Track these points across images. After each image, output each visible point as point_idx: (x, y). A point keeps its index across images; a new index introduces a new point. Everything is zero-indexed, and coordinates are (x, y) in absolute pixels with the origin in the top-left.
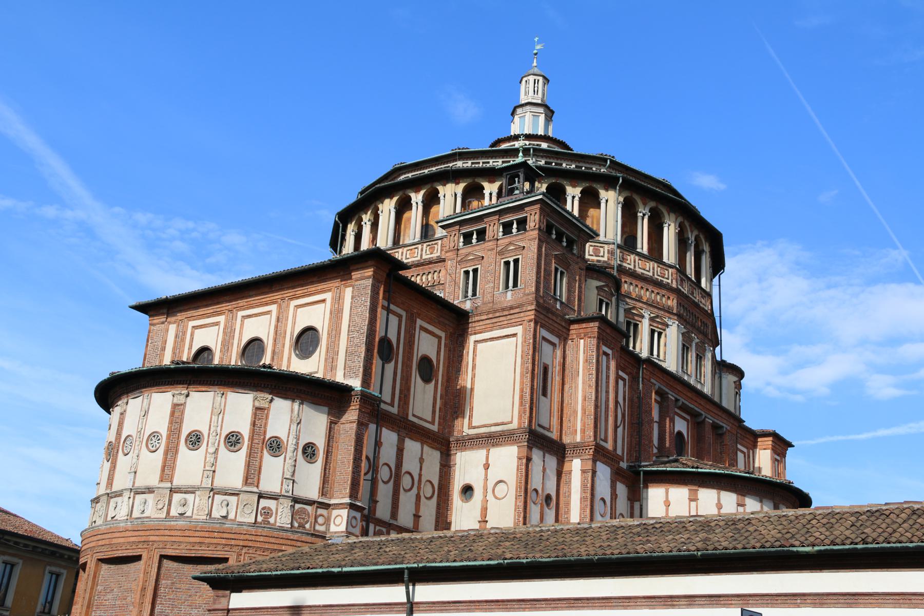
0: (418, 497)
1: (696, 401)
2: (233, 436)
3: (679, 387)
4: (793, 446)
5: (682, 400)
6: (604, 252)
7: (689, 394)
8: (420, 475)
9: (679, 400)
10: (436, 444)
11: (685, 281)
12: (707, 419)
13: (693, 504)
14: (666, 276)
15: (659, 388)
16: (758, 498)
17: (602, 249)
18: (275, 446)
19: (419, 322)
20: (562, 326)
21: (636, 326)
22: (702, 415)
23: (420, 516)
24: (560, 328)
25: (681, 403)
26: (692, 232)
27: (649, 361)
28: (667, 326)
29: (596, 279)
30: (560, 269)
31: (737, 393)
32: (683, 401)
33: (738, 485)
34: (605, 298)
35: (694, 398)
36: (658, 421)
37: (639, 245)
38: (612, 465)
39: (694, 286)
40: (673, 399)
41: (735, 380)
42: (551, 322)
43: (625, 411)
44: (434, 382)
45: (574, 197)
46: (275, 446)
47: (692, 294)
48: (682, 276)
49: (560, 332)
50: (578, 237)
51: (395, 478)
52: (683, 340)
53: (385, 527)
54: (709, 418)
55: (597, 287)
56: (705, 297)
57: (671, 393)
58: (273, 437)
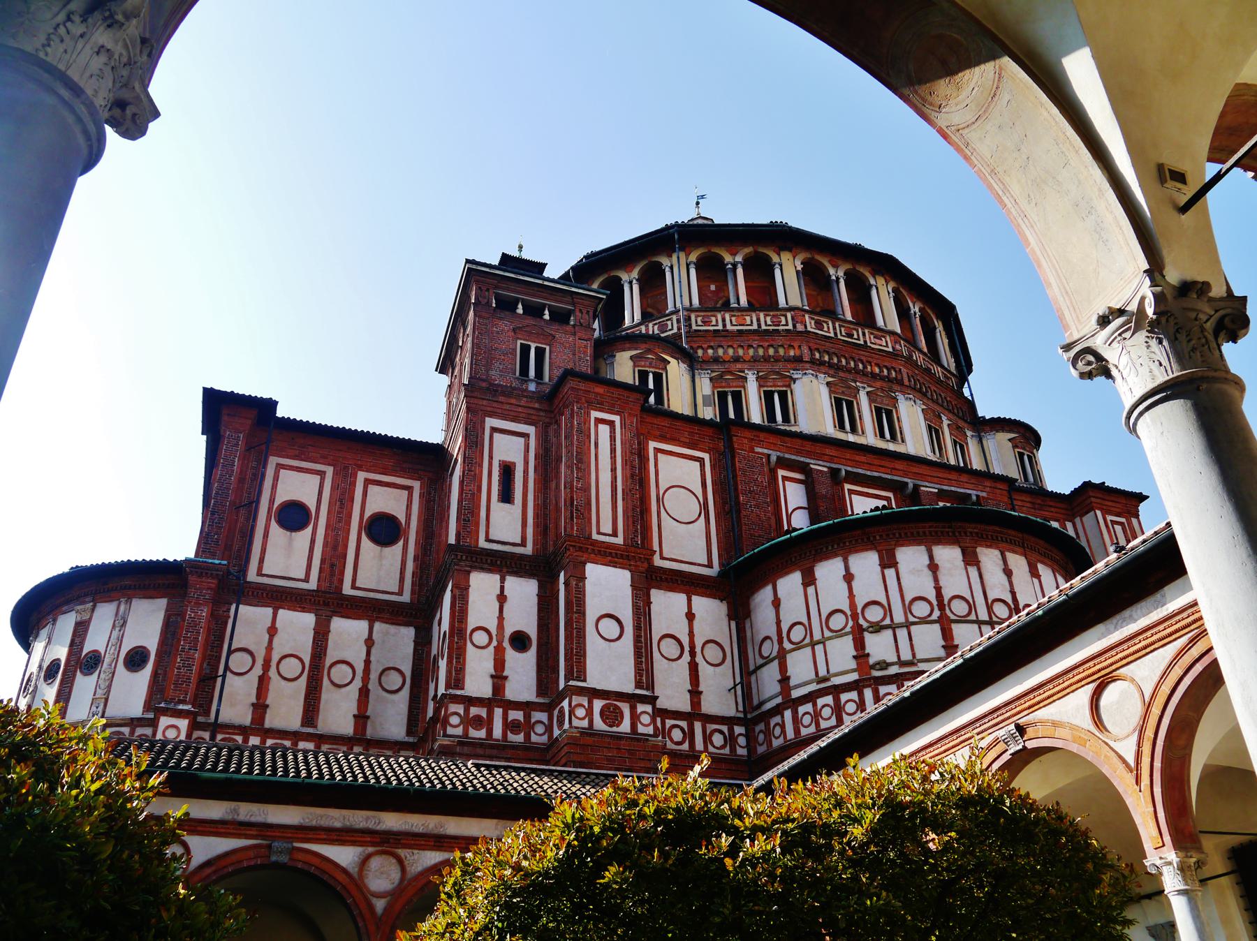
0: (364, 693)
1: (883, 467)
2: (54, 665)
4: (1147, 497)
5: (844, 469)
6: (672, 324)
7: (863, 459)
8: (367, 662)
10: (401, 618)
11: (826, 322)
12: (922, 488)
13: (811, 590)
14: (784, 322)
15: (778, 458)
16: (923, 548)
17: (669, 323)
18: (92, 663)
19: (361, 476)
20: (534, 408)
21: (737, 397)
22: (907, 483)
23: (368, 717)
24: (532, 412)
25: (843, 473)
26: (836, 267)
27: (768, 431)
28: (795, 380)
29: (629, 349)
30: (533, 346)
31: (1021, 455)
32: (849, 469)
33: (875, 537)
34: (649, 367)
35: (876, 462)
36: (806, 506)
37: (732, 300)
38: (630, 565)
39: (852, 326)
40: (825, 469)
41: (1010, 437)
42: (508, 407)
43: (705, 498)
44: (401, 543)
45: (631, 283)
46: (92, 663)
47: (851, 336)
48: (816, 318)
49: (534, 417)
50: (573, 304)
51: (309, 671)
52: (831, 392)
53: (287, 739)
54: (924, 486)
55: (632, 358)
56: (884, 337)
57: (812, 461)
58: (90, 652)
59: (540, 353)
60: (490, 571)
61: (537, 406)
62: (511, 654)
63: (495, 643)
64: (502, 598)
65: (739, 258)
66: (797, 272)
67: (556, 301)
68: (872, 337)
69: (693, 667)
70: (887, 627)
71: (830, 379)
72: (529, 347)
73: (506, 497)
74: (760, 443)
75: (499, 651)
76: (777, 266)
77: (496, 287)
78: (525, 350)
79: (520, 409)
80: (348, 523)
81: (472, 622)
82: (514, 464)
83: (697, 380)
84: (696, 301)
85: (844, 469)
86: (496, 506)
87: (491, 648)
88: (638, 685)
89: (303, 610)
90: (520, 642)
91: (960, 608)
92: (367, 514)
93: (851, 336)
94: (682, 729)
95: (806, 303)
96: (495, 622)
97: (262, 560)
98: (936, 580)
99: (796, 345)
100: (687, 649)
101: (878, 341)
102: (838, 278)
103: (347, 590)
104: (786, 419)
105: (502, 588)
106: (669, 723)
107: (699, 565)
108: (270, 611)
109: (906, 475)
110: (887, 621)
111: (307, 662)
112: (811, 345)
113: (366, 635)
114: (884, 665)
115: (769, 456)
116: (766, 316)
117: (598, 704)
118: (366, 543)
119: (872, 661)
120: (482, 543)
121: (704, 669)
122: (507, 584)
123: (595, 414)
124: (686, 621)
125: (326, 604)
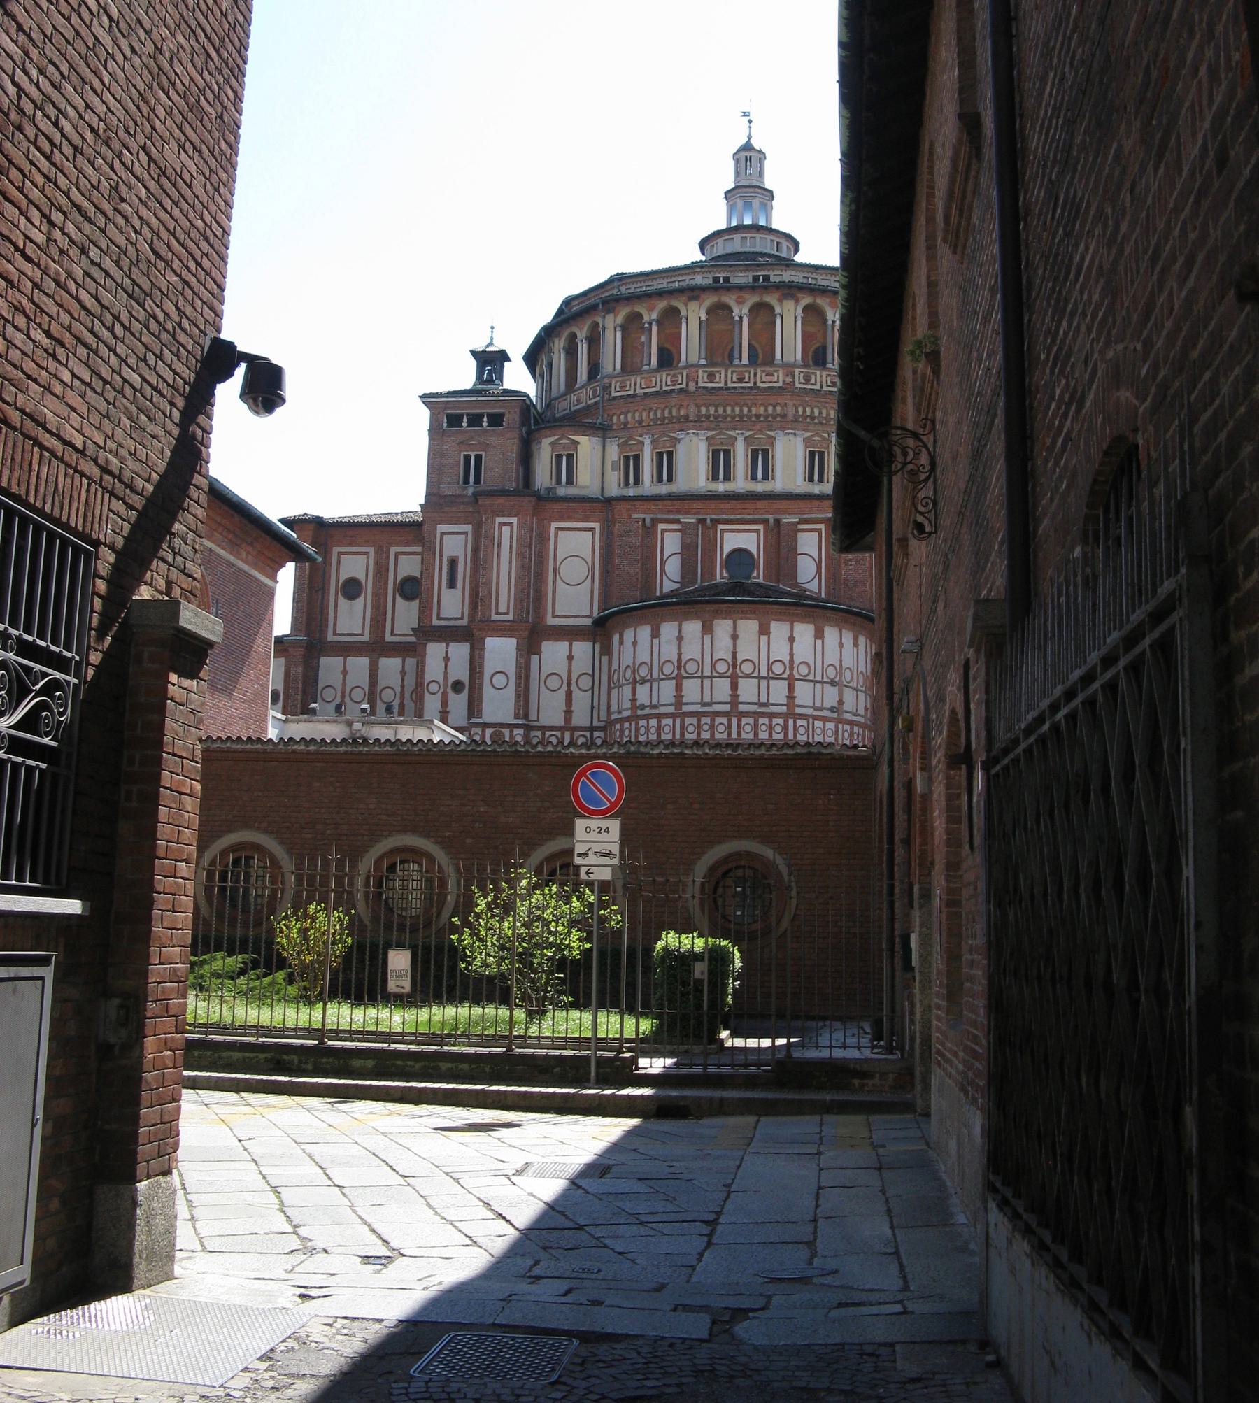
3: (697, 505)
8: (403, 687)
9: (705, 520)
19: (393, 550)
28: (679, 440)
30: (473, 455)
32: (714, 517)
59: (478, 458)
60: (440, 641)
61: (471, 509)
62: (452, 696)
63: (442, 690)
64: (447, 659)
65: (654, 316)
66: (701, 322)
67: (493, 408)
68: (764, 375)
69: (569, 695)
70: (648, 681)
71: (711, 433)
72: (470, 456)
73: (452, 584)
74: (636, 510)
75: (445, 695)
76: (684, 320)
77: (446, 409)
78: (467, 458)
79: (459, 515)
80: (386, 588)
81: (428, 678)
82: (457, 557)
83: (607, 448)
84: (618, 366)
85: (708, 517)
86: (446, 592)
87: (440, 694)
88: (517, 717)
89: (361, 656)
90: (457, 687)
91: (692, 667)
92: (399, 578)
93: (741, 380)
94: (557, 737)
95: (703, 355)
96: (442, 676)
97: (335, 625)
98: (680, 647)
99: (685, 403)
100: (565, 681)
101: (769, 379)
102: (741, 317)
103: (389, 638)
104: (670, 479)
105: (447, 652)
106: (548, 733)
107: (583, 617)
108: (342, 659)
109: (767, 512)
110: (649, 677)
111: (367, 689)
112: (698, 401)
113: (400, 668)
114: (643, 707)
115: (644, 520)
116: (667, 375)
117: (489, 732)
118: (399, 599)
119: (638, 703)
120: (435, 622)
121: (577, 694)
122: (450, 649)
123: (499, 520)
124: (566, 662)
125: (373, 651)
